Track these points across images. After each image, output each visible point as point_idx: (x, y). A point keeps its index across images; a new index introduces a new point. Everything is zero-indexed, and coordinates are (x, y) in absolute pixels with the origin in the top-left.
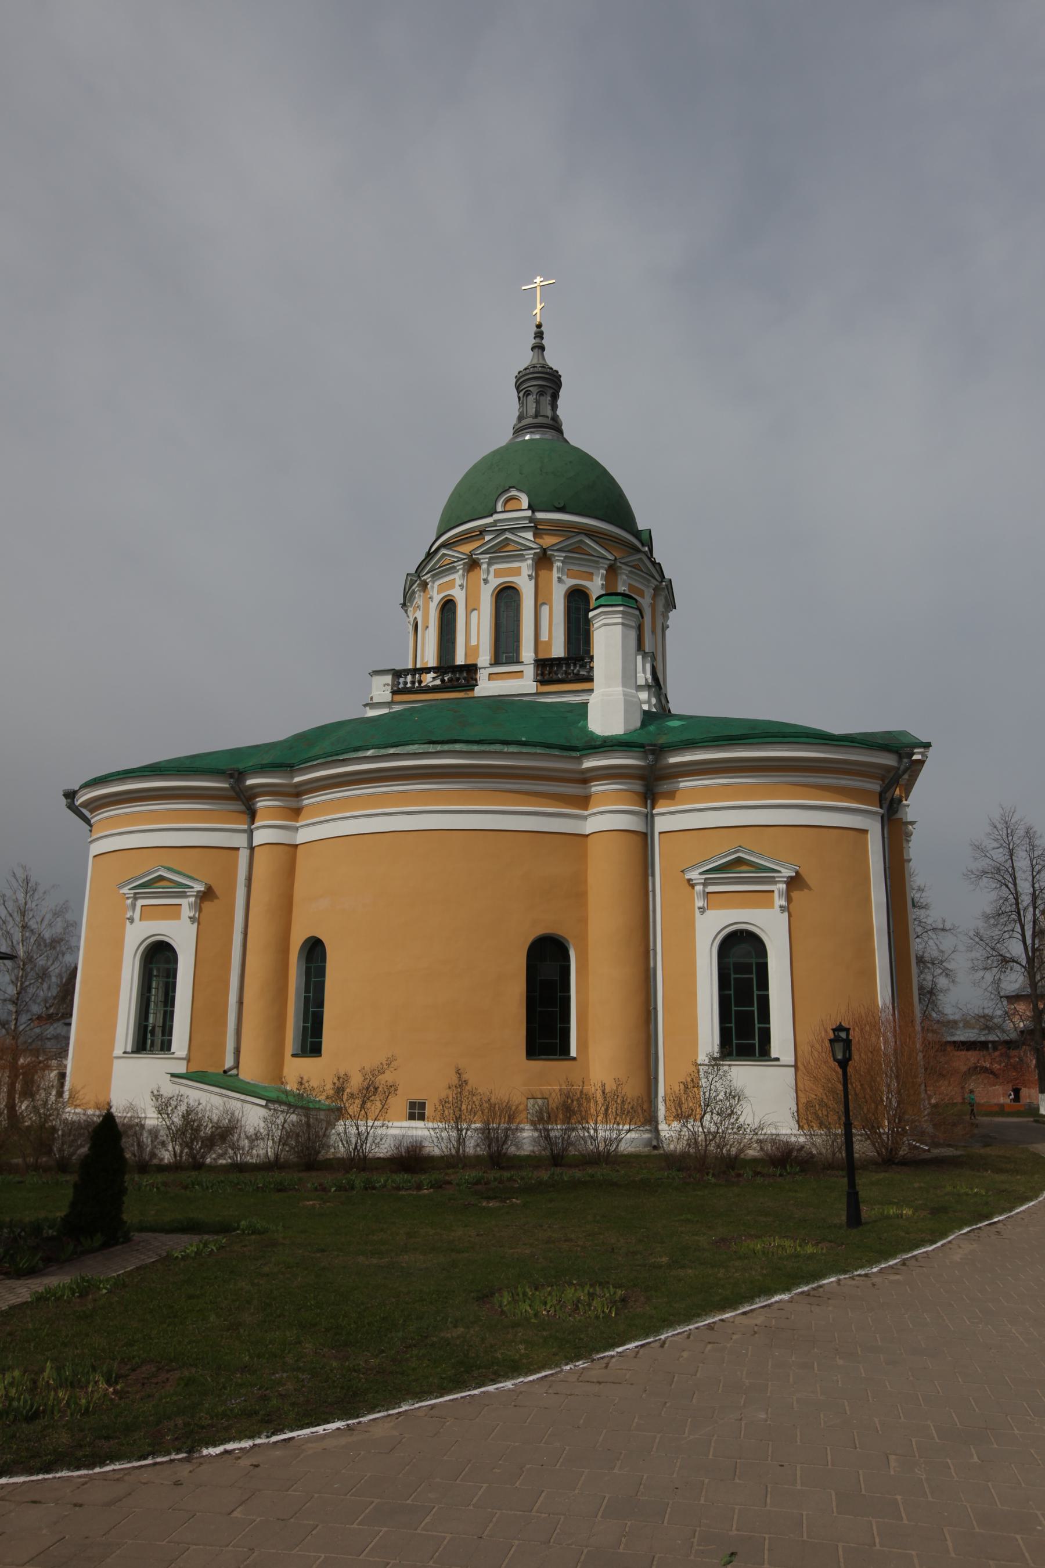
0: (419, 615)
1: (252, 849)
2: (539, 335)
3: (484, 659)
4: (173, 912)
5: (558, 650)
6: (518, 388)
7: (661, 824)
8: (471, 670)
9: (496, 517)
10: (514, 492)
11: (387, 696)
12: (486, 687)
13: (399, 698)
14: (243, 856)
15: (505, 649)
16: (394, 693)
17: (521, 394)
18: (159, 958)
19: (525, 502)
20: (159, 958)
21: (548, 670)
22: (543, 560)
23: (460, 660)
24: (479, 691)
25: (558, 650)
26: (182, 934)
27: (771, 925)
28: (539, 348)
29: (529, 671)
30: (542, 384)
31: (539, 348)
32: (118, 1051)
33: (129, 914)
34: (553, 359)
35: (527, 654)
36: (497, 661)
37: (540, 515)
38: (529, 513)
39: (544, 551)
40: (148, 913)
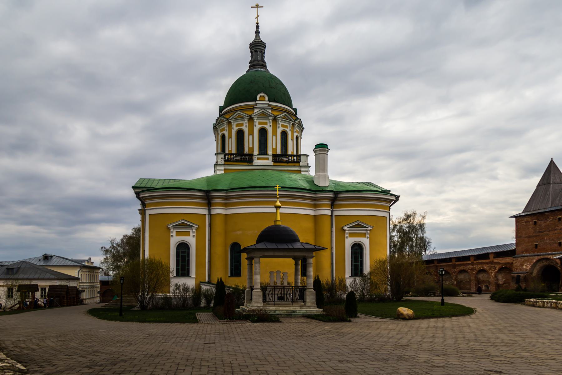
0: (226, 133)
1: (210, 214)
2: (258, 27)
3: (256, 152)
4: (188, 234)
5: (279, 152)
6: (251, 48)
8: (251, 155)
9: (257, 102)
10: (262, 94)
11: (223, 162)
12: (256, 162)
13: (227, 163)
14: (207, 216)
15: (263, 150)
17: (253, 51)
18: (183, 248)
19: (267, 99)
20: (183, 248)
21: (277, 158)
22: (275, 120)
24: (254, 163)
25: (279, 152)
26: (191, 240)
28: (257, 32)
29: (271, 158)
30: (257, 47)
31: (257, 32)
32: (171, 276)
33: (171, 234)
34: (263, 38)
35: (270, 152)
36: (259, 154)
37: (271, 103)
38: (268, 102)
39: (275, 117)
40: (178, 234)
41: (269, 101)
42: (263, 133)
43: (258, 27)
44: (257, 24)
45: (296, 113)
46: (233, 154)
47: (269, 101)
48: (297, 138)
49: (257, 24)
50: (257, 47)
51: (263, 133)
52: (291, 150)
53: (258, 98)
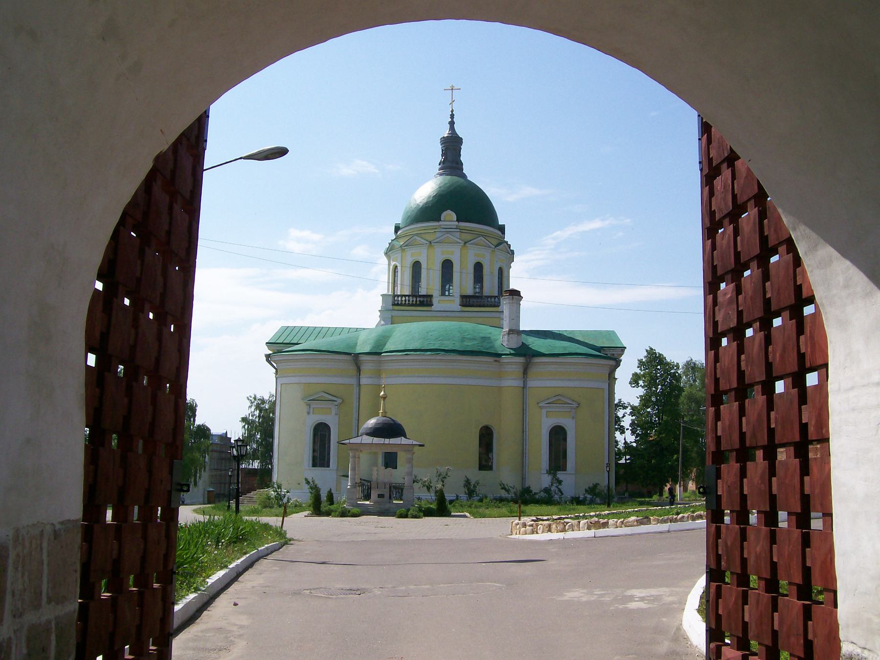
2: (452, 116)
7: (530, 383)
9: (441, 223)
13: (396, 308)
16: (394, 305)
19: (455, 218)
21: (467, 301)
23: (423, 291)
25: (469, 291)
27: (569, 425)
28: (452, 123)
29: (458, 300)
30: (452, 146)
31: (452, 123)
34: (460, 132)
37: (463, 224)
41: (458, 220)
42: (447, 266)
43: (452, 116)
44: (452, 111)
45: (503, 233)
46: (405, 296)
47: (458, 220)
48: (501, 271)
49: (452, 111)
50: (452, 146)
51: (447, 266)
52: (490, 287)
53: (442, 219)
